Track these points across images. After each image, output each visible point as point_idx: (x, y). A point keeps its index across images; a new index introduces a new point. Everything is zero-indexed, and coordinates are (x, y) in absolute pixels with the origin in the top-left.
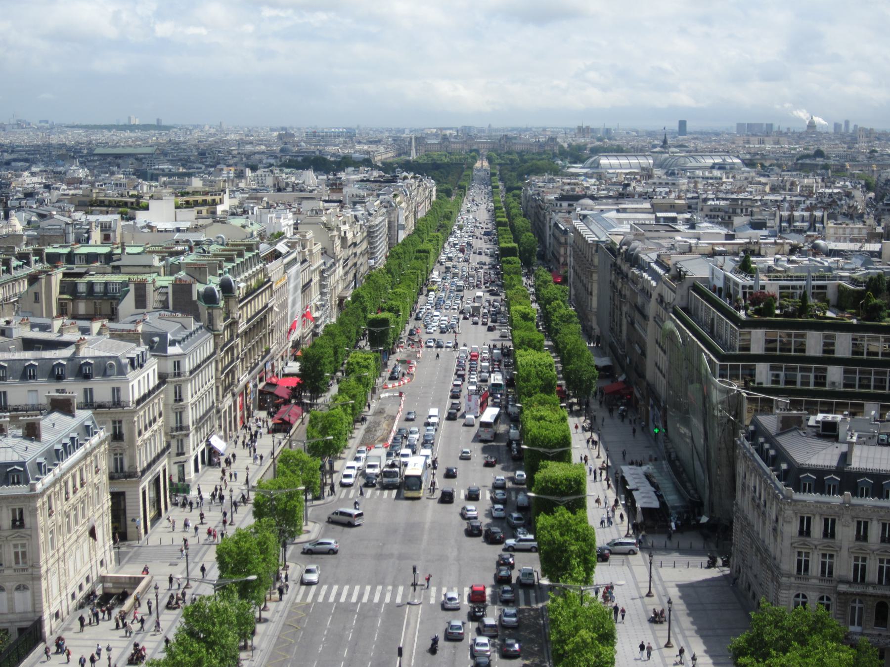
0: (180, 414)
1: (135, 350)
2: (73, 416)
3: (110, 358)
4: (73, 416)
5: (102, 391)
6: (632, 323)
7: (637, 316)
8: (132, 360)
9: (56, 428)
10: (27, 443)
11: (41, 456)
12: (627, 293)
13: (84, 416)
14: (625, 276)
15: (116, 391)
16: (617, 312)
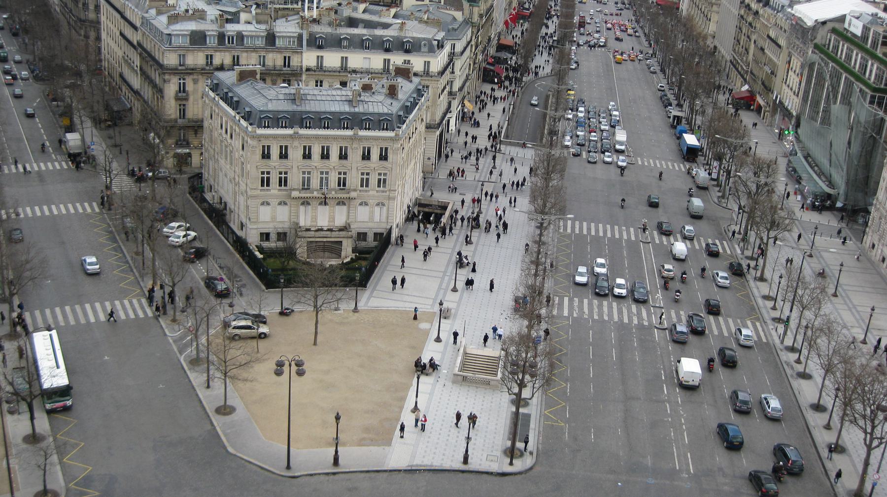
0: (451, 83)
1: (440, 36)
2: (411, 81)
3: (424, 39)
4: (411, 81)
5: (417, 63)
6: (762, 49)
7: (767, 45)
8: (438, 41)
9: (406, 88)
10: (389, 101)
11: (400, 109)
12: (758, 26)
13: (416, 80)
14: (756, 13)
15: (427, 64)
16: (743, 38)
